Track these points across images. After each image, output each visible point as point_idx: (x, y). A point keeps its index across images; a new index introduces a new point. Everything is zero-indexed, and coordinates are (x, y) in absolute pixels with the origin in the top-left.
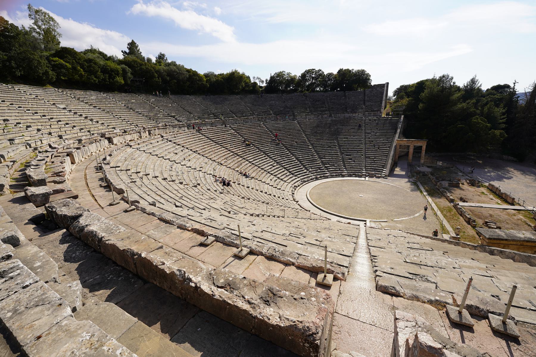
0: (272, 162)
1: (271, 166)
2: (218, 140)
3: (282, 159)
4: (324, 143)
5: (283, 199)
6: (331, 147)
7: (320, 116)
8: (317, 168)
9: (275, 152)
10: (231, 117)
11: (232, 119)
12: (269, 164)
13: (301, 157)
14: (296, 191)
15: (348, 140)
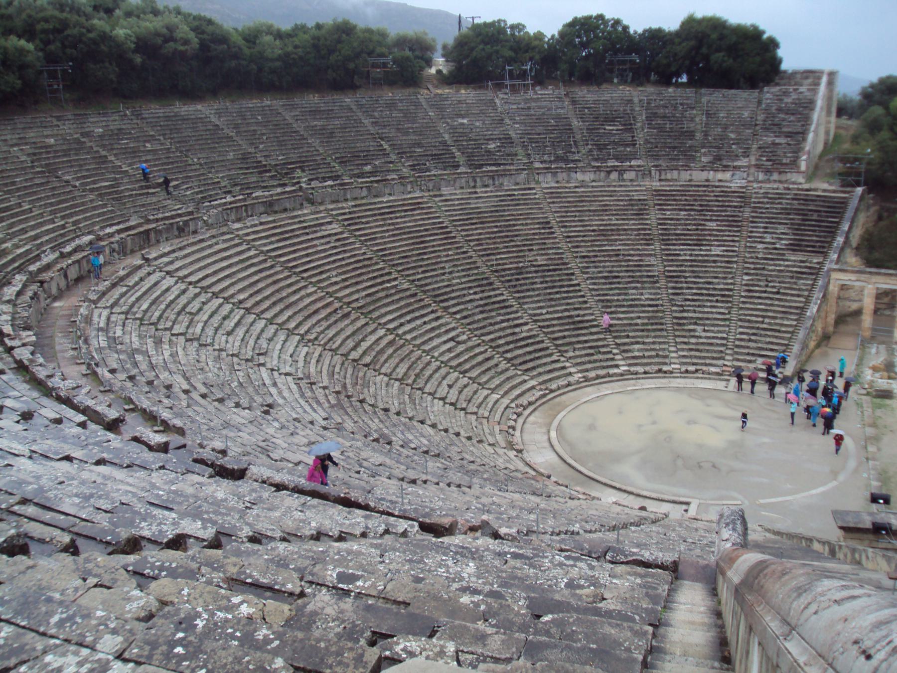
0: (453, 329)
1: (452, 344)
2: (295, 259)
3: (485, 319)
4: (620, 266)
5: (480, 442)
6: (638, 282)
7: (614, 176)
8: (591, 348)
9: (464, 295)
10: (330, 178)
11: (332, 186)
12: (445, 338)
13: (544, 311)
14: (521, 420)
15: (692, 261)
